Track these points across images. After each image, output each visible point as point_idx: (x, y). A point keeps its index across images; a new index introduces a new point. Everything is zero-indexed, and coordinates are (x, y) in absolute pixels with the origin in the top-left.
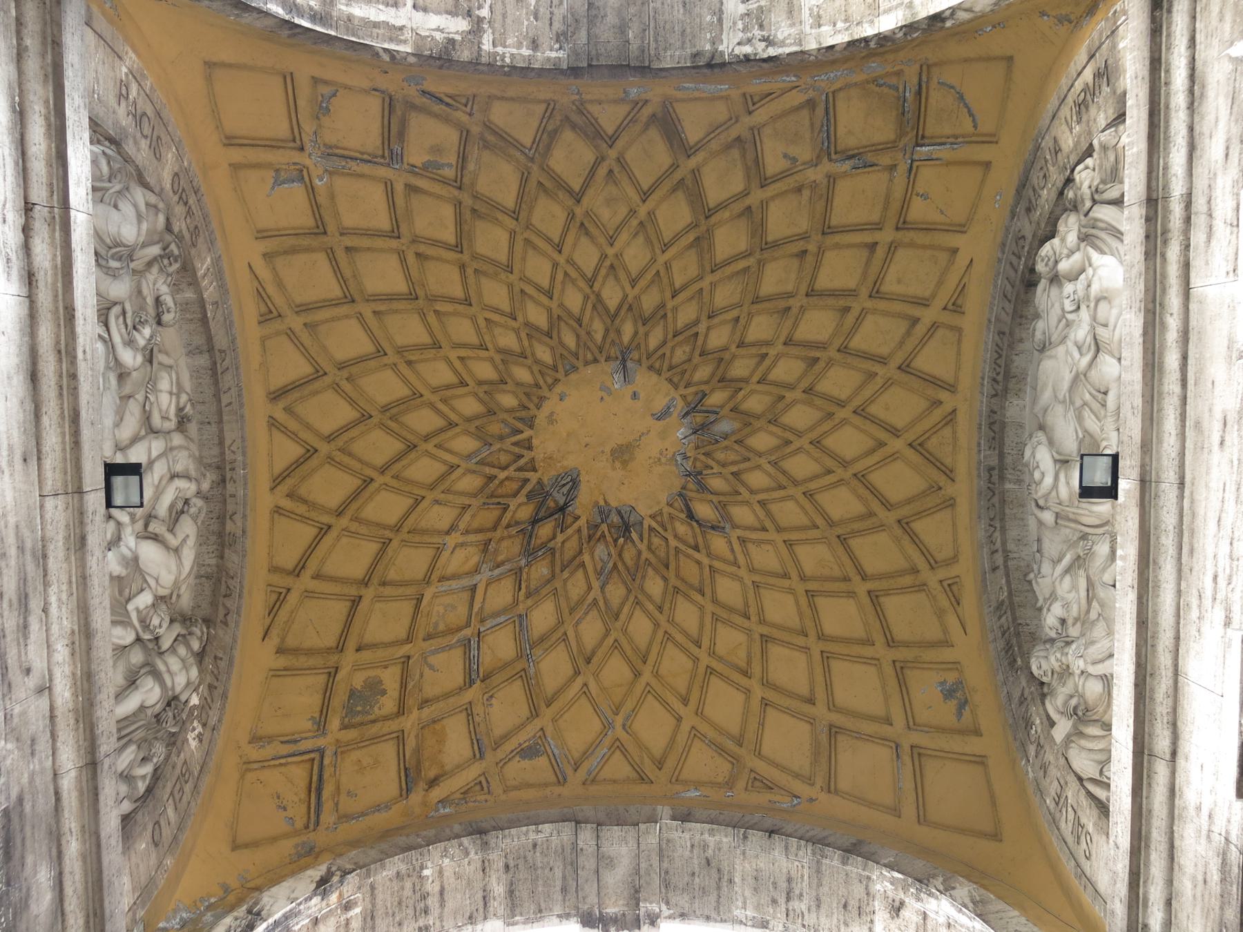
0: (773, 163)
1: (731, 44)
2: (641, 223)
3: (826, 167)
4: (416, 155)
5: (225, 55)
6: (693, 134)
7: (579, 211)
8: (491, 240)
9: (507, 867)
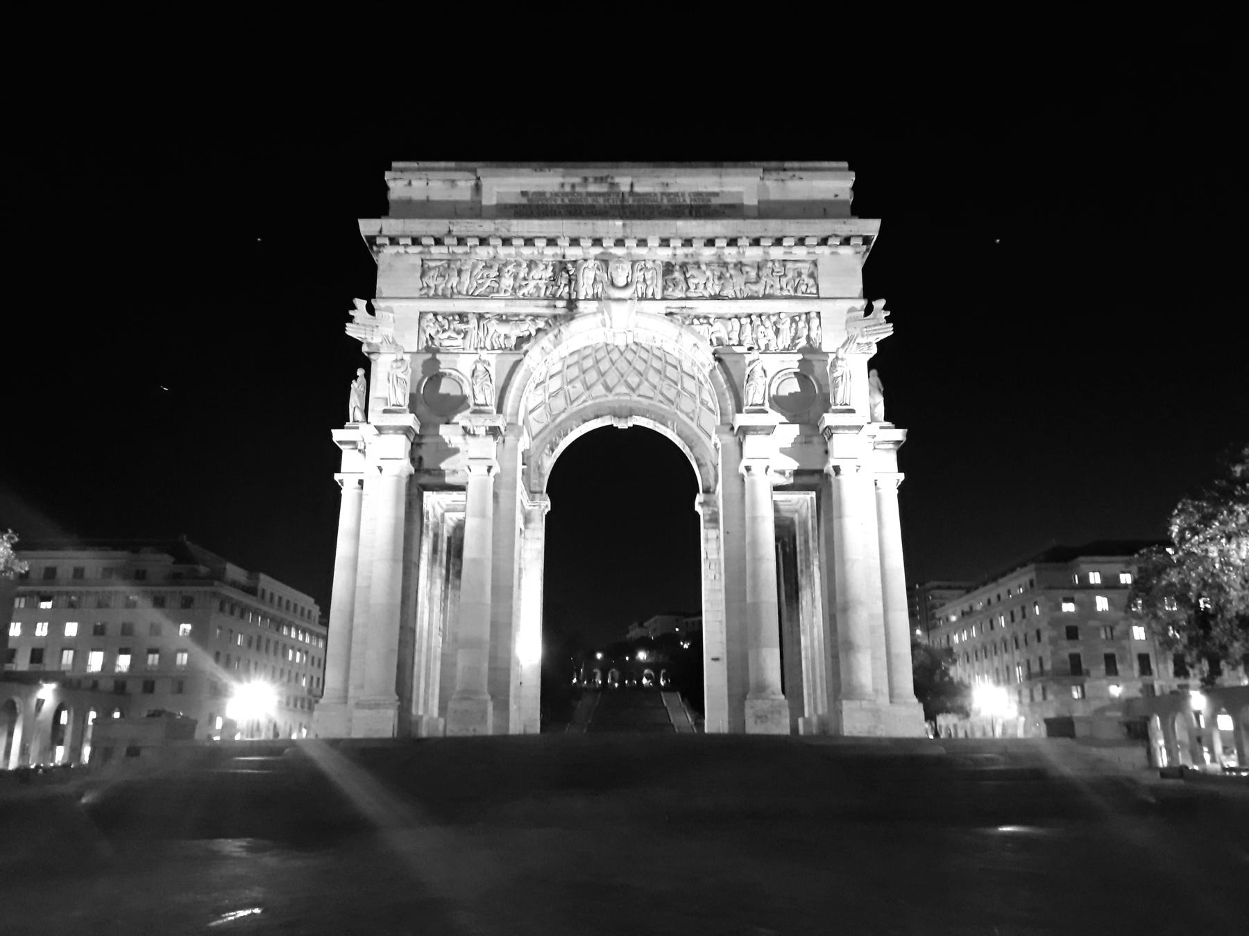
0: (578, 385)
4: (674, 392)
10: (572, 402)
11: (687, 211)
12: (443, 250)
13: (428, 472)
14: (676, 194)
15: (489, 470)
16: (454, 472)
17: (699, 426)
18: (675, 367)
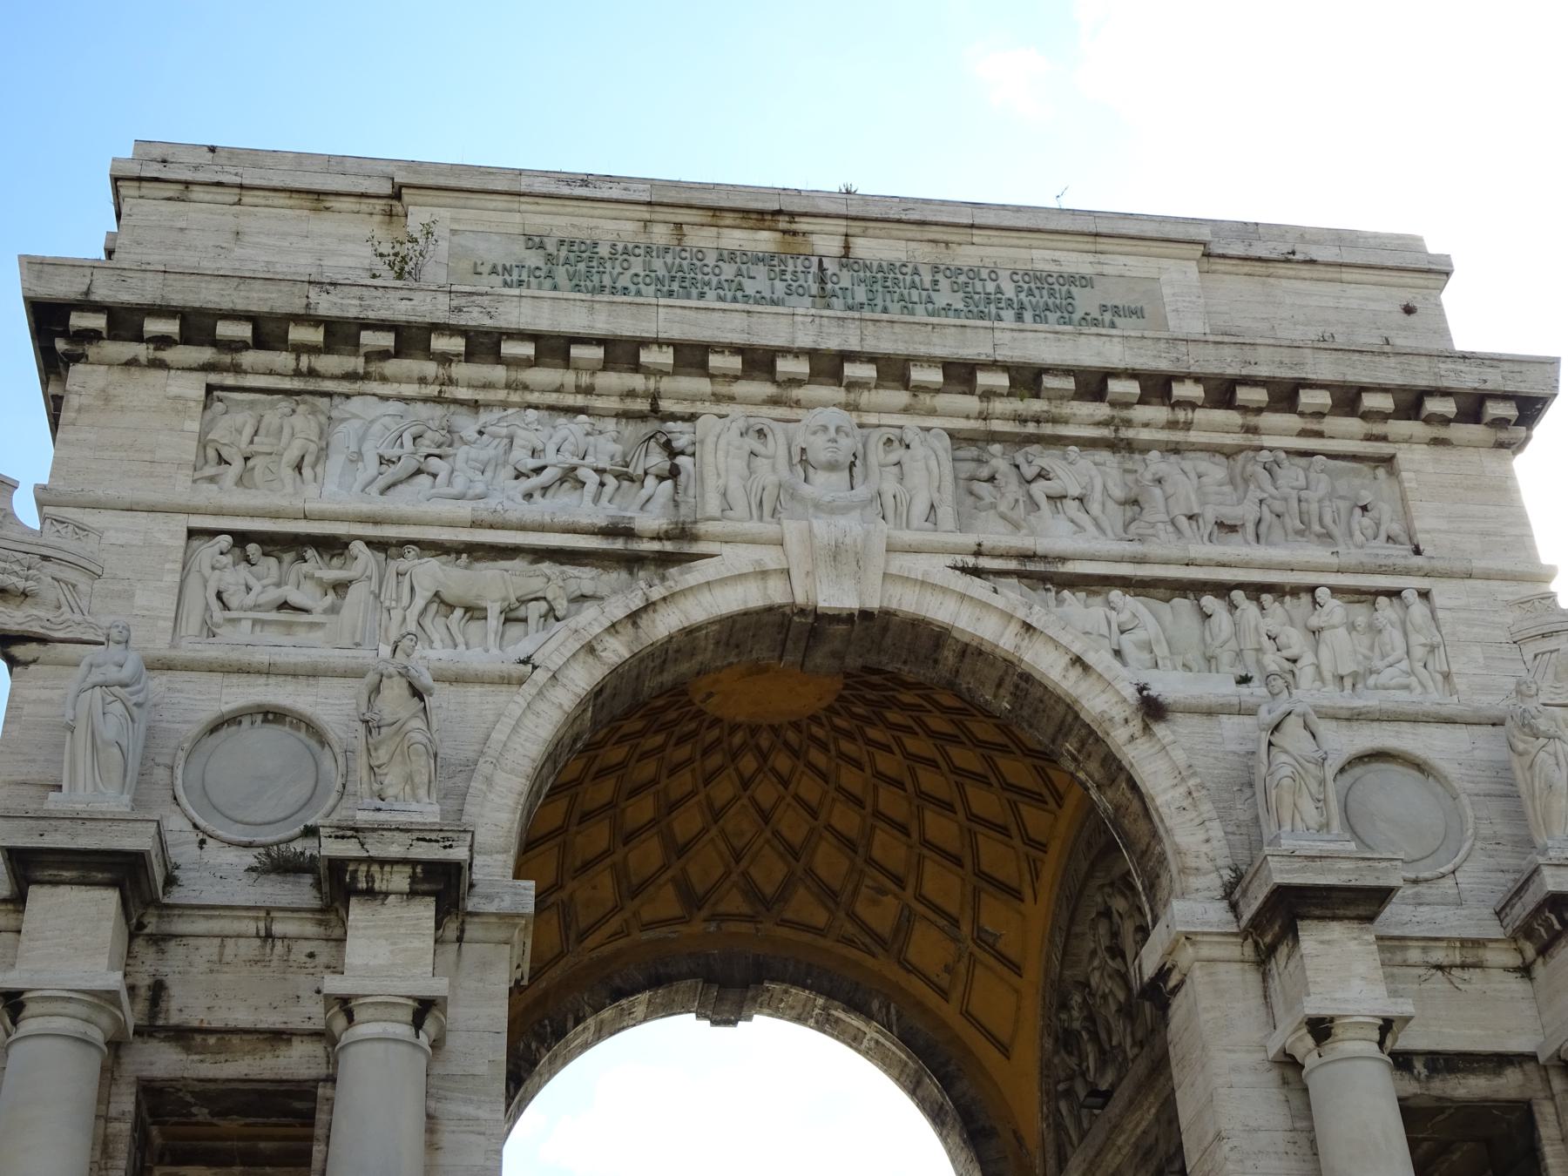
1: (644, 997)
2: (716, 822)
3: (563, 895)
4: (890, 904)
5: (995, 1055)
6: (669, 892)
7: (768, 834)
8: (846, 819)
9: (936, 661)
10: (582, 936)
11: (1008, 315)
12: (284, 360)
13: (182, 1036)
14: (974, 273)
15: (417, 1023)
16: (279, 1037)
17: (967, 1014)
18: (904, 829)
